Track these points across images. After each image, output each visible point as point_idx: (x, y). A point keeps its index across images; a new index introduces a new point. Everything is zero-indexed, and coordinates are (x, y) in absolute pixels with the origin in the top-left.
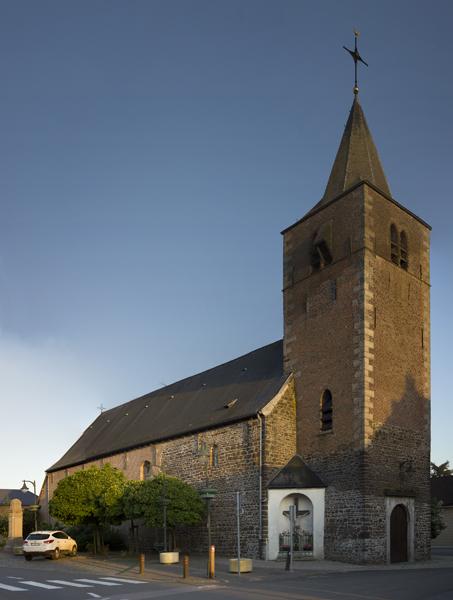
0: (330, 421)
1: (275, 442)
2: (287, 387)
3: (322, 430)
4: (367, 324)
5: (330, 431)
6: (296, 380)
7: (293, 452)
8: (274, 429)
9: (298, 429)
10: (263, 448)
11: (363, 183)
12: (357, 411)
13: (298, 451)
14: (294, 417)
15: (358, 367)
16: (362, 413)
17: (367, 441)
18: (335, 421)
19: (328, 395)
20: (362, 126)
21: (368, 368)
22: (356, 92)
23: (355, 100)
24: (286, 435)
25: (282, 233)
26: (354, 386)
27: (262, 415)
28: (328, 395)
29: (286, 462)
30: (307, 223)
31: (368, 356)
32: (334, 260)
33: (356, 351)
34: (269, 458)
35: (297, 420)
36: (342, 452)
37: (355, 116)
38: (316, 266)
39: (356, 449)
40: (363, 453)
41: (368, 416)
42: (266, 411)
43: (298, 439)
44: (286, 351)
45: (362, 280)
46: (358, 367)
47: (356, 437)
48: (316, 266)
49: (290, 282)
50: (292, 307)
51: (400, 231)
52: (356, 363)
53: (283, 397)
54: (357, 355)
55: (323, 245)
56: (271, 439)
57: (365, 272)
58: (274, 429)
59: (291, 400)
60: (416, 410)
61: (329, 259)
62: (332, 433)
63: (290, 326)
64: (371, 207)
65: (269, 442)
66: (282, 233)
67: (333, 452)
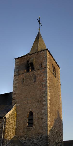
0: (32, 123)
1: (8, 129)
2: (14, 108)
3: (28, 126)
4: (48, 90)
5: (31, 127)
6: (17, 107)
7: (14, 134)
8: (9, 124)
9: (16, 125)
10: (4, 131)
11: (47, 49)
12: (44, 120)
13: (16, 134)
14: (15, 120)
15: (45, 104)
16: (47, 121)
17: (49, 132)
18: (34, 124)
19: (31, 114)
20: (41, 38)
21: (49, 105)
22: (39, 30)
23: (39, 32)
24: (12, 127)
25: (15, 59)
26: (43, 111)
27: (5, 118)
28: (31, 114)
29: (11, 138)
30: (25, 57)
31: (49, 101)
32: (35, 69)
33: (44, 99)
34: (6, 136)
35: (17, 122)
36: (37, 136)
37: (39, 35)
38: (28, 71)
39: (44, 135)
40: (47, 137)
41: (49, 123)
42: (7, 116)
43: (16, 129)
44: (13, 96)
45: (47, 77)
46: (45, 104)
47: (44, 130)
48: (28, 71)
49: (17, 74)
50: (17, 82)
51: (54, 66)
52: (44, 103)
53: (12, 112)
54: (45, 100)
55: (32, 64)
56: (7, 128)
57: (48, 74)
58: (9, 124)
59: (15, 114)
60: (59, 123)
61: (33, 69)
62: (33, 128)
63: (16, 88)
64: (48, 57)
65: (6, 129)
66: (15, 59)
67: (33, 136)
